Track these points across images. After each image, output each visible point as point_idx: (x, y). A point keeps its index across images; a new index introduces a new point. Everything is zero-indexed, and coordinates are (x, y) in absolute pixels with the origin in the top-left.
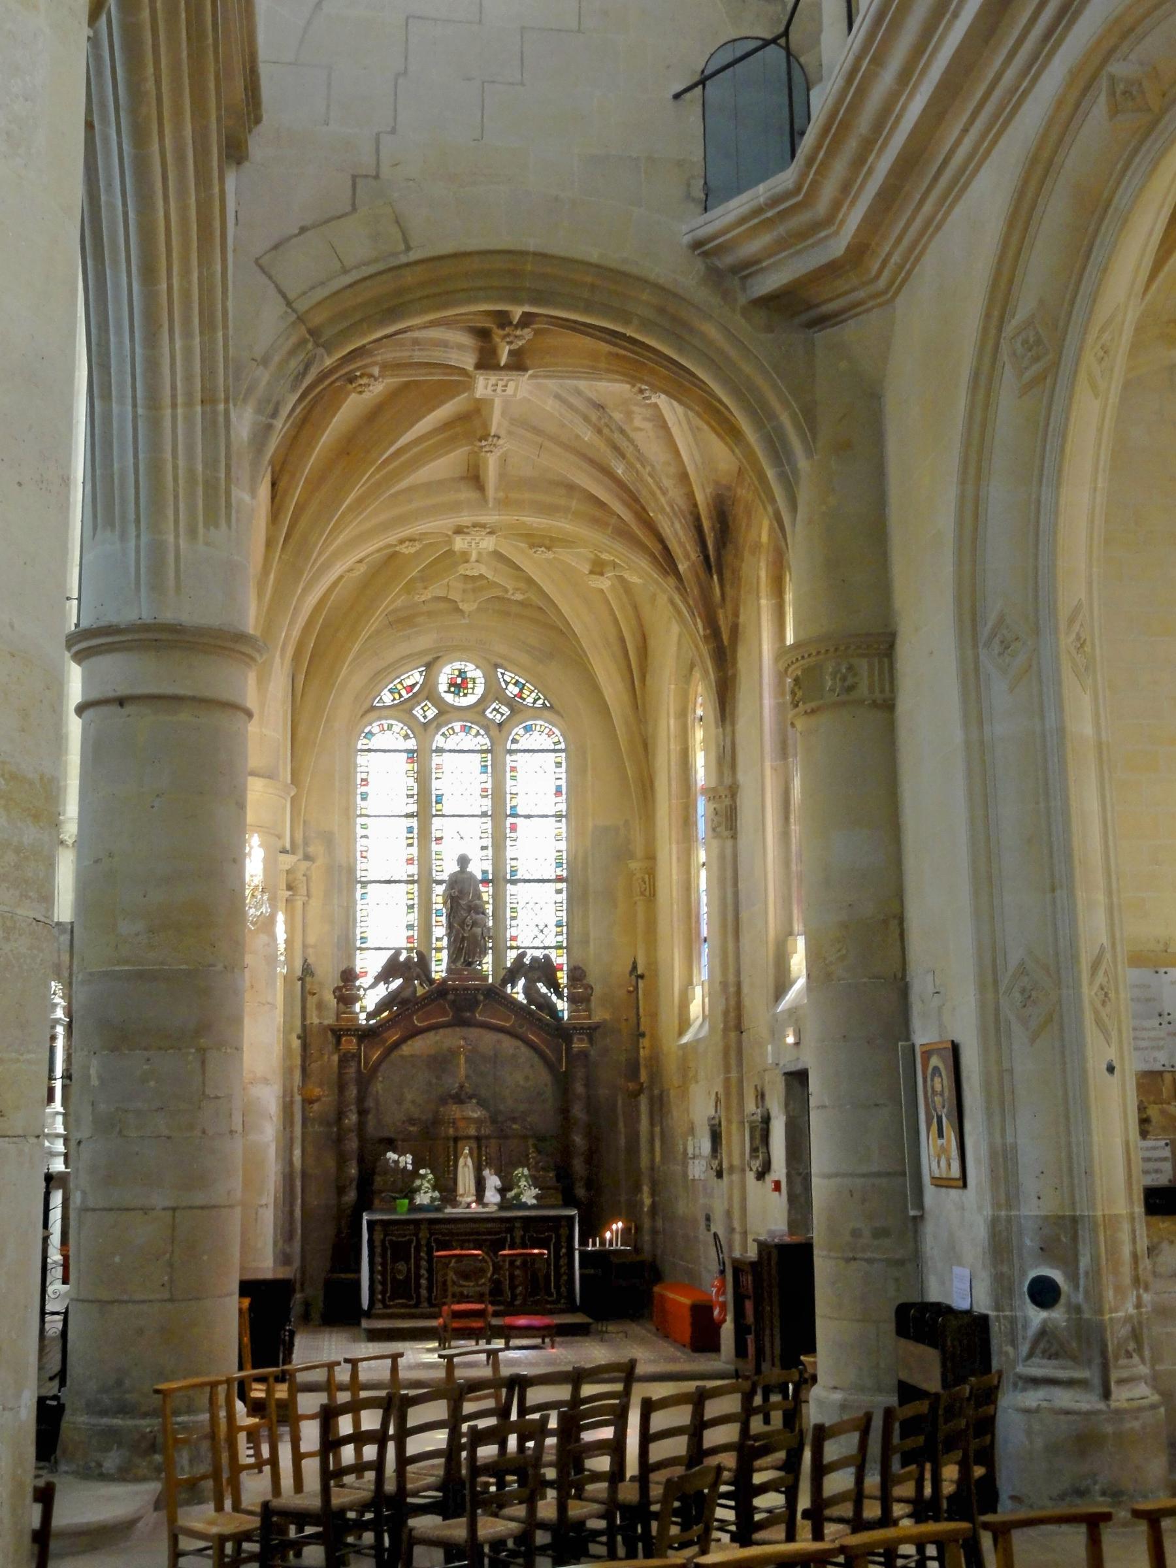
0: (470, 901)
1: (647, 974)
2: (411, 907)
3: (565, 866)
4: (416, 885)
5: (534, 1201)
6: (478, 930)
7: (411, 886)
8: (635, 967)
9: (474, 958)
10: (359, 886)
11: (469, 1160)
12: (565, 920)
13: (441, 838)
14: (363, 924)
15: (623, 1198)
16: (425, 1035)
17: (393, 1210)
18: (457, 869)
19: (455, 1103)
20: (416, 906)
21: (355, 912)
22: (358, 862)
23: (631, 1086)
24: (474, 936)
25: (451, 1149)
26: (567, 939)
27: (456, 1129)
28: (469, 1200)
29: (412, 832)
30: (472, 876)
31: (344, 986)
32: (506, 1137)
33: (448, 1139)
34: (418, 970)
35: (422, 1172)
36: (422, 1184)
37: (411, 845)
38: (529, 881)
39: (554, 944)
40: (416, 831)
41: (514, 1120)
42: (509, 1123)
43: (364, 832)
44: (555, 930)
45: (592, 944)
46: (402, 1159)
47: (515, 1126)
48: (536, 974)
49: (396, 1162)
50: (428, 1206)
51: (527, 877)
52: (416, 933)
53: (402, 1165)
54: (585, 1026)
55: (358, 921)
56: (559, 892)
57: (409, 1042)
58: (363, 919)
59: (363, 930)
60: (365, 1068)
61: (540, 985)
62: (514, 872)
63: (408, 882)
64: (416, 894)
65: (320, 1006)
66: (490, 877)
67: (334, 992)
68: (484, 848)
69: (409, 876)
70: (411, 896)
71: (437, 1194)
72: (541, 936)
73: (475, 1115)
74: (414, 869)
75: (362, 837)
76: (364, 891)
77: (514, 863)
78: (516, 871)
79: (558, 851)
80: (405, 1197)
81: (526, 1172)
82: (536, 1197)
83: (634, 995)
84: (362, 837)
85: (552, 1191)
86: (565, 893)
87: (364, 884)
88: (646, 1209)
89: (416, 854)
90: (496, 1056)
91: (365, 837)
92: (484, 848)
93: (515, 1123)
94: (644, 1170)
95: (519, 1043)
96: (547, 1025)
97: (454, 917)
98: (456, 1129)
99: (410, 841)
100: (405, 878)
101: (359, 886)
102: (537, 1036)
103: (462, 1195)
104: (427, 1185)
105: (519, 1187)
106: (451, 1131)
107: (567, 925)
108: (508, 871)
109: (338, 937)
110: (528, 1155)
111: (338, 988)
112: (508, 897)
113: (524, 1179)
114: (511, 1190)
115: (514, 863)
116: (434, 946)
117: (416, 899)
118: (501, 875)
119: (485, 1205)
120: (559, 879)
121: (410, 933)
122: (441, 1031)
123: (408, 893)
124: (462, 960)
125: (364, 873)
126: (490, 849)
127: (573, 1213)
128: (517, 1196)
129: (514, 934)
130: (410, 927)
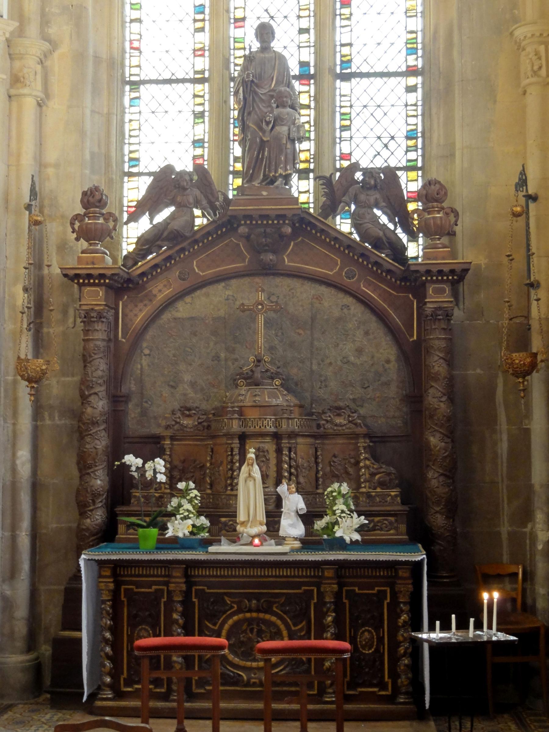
0: (273, 90)
1: (542, 194)
2: (201, 115)
3: (420, 53)
4: (207, 84)
5: (357, 537)
6: (284, 129)
7: (199, 87)
8: (523, 182)
9: (276, 171)
10: (127, 88)
11: (256, 468)
12: (420, 129)
13: (243, 19)
14: (133, 140)
15: (505, 529)
16: (210, 289)
17: (134, 544)
18: (256, 45)
19: (248, 385)
20: (207, 114)
21: (123, 123)
22: (127, 55)
23: (519, 358)
24: (278, 139)
25: (236, 451)
26: (423, 156)
27: (244, 421)
28: (254, 530)
29: (203, 13)
30: (280, 59)
31: (85, 215)
32: (324, 436)
33: (229, 436)
34: (197, 192)
35: (181, 485)
36: (180, 506)
37: (202, 29)
38: (368, 75)
39: (404, 163)
40: (207, 11)
41: (338, 410)
42: (329, 415)
43: (135, 15)
44: (404, 143)
45: (458, 154)
46: (149, 465)
47: (338, 420)
48: (375, 196)
49: (141, 470)
50: (185, 538)
51: (365, 69)
52: (206, 150)
53: (149, 475)
54: (446, 269)
55: (127, 136)
56: (411, 89)
57: (188, 299)
58: (132, 133)
59: (133, 148)
60: (124, 335)
61: (378, 212)
62: (347, 62)
63: (194, 81)
64: (207, 97)
65: (62, 247)
66: (312, 72)
67: (72, 224)
68: (302, 31)
69: (196, 72)
70: (199, 100)
71: (203, 521)
72: (385, 153)
73: (274, 402)
74: (203, 63)
75: (132, 21)
76: (133, 95)
77: (346, 50)
78: (350, 61)
79: (412, 32)
80: (152, 524)
81: (345, 488)
82: (360, 530)
83: (523, 218)
84: (132, 21)
85: (392, 519)
86: (420, 91)
87: (135, 85)
88: (540, 547)
89: (207, 43)
90: (313, 319)
91: (139, 21)
92: (302, 31)
93: (339, 415)
94: (537, 488)
95: (349, 300)
96: (389, 272)
97: (249, 114)
98: (244, 421)
99: (199, 25)
100: (191, 75)
101: (127, 88)
102: (376, 289)
103: (243, 523)
104: (189, 507)
105: (334, 513)
106: (235, 426)
107: (423, 136)
108: (338, 62)
109: (92, 154)
110: (357, 463)
111: (77, 217)
112: (338, 98)
113: (341, 500)
114: (321, 516)
115: (346, 50)
116: (231, 169)
117: (207, 104)
118: (327, 64)
119: (280, 541)
120: (412, 72)
121: (199, 151)
122: (234, 282)
123: (195, 96)
124: (262, 176)
125: (135, 71)
126: (312, 31)
127: (419, 558)
128: (330, 528)
129: (346, 151)
130: (197, 143)
